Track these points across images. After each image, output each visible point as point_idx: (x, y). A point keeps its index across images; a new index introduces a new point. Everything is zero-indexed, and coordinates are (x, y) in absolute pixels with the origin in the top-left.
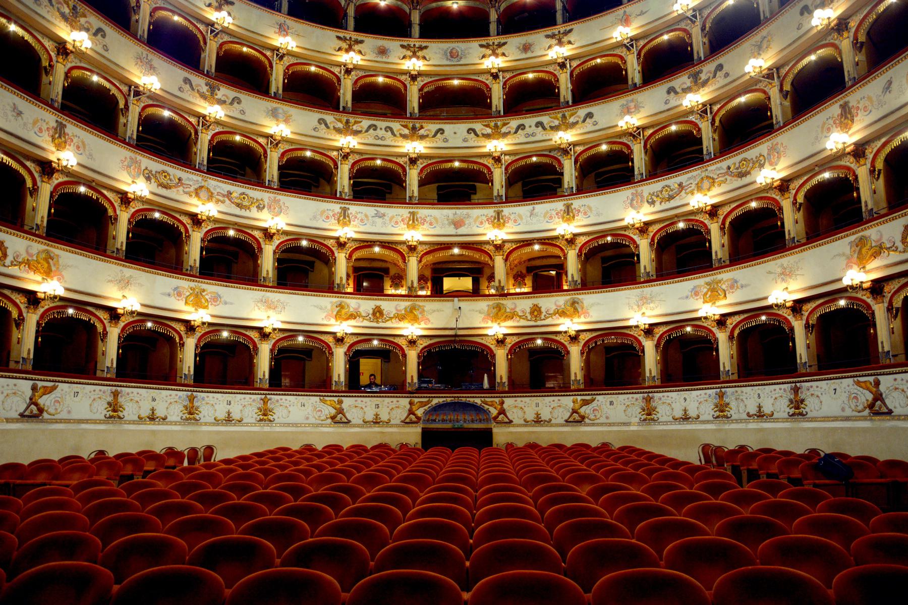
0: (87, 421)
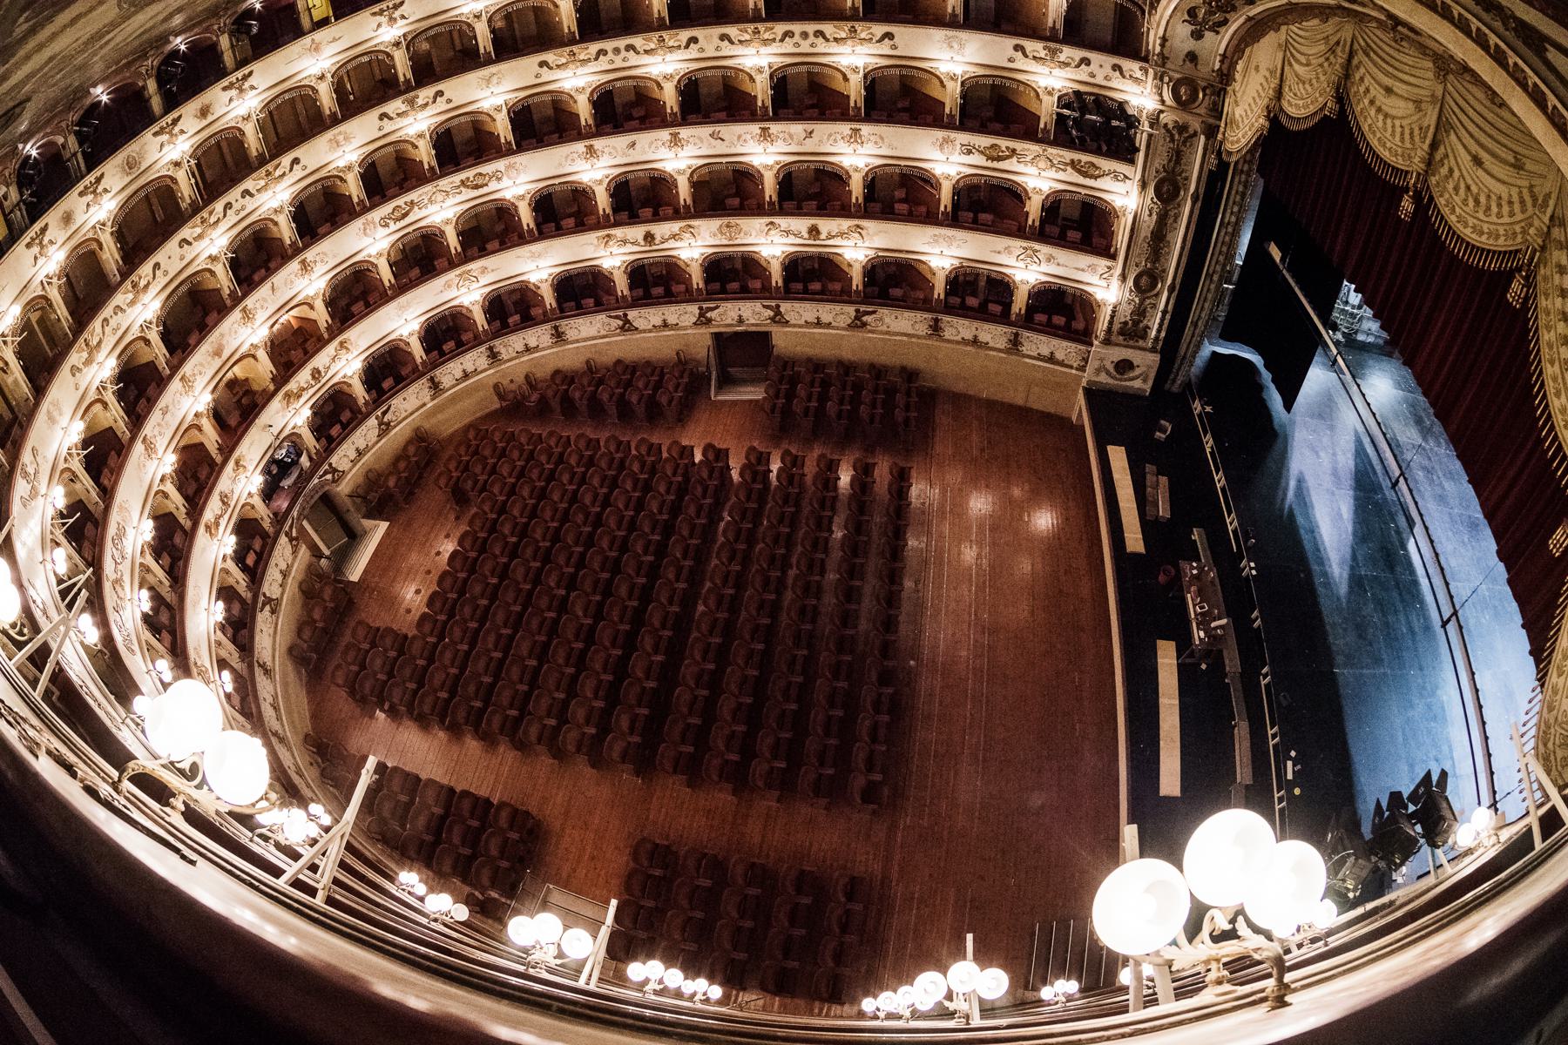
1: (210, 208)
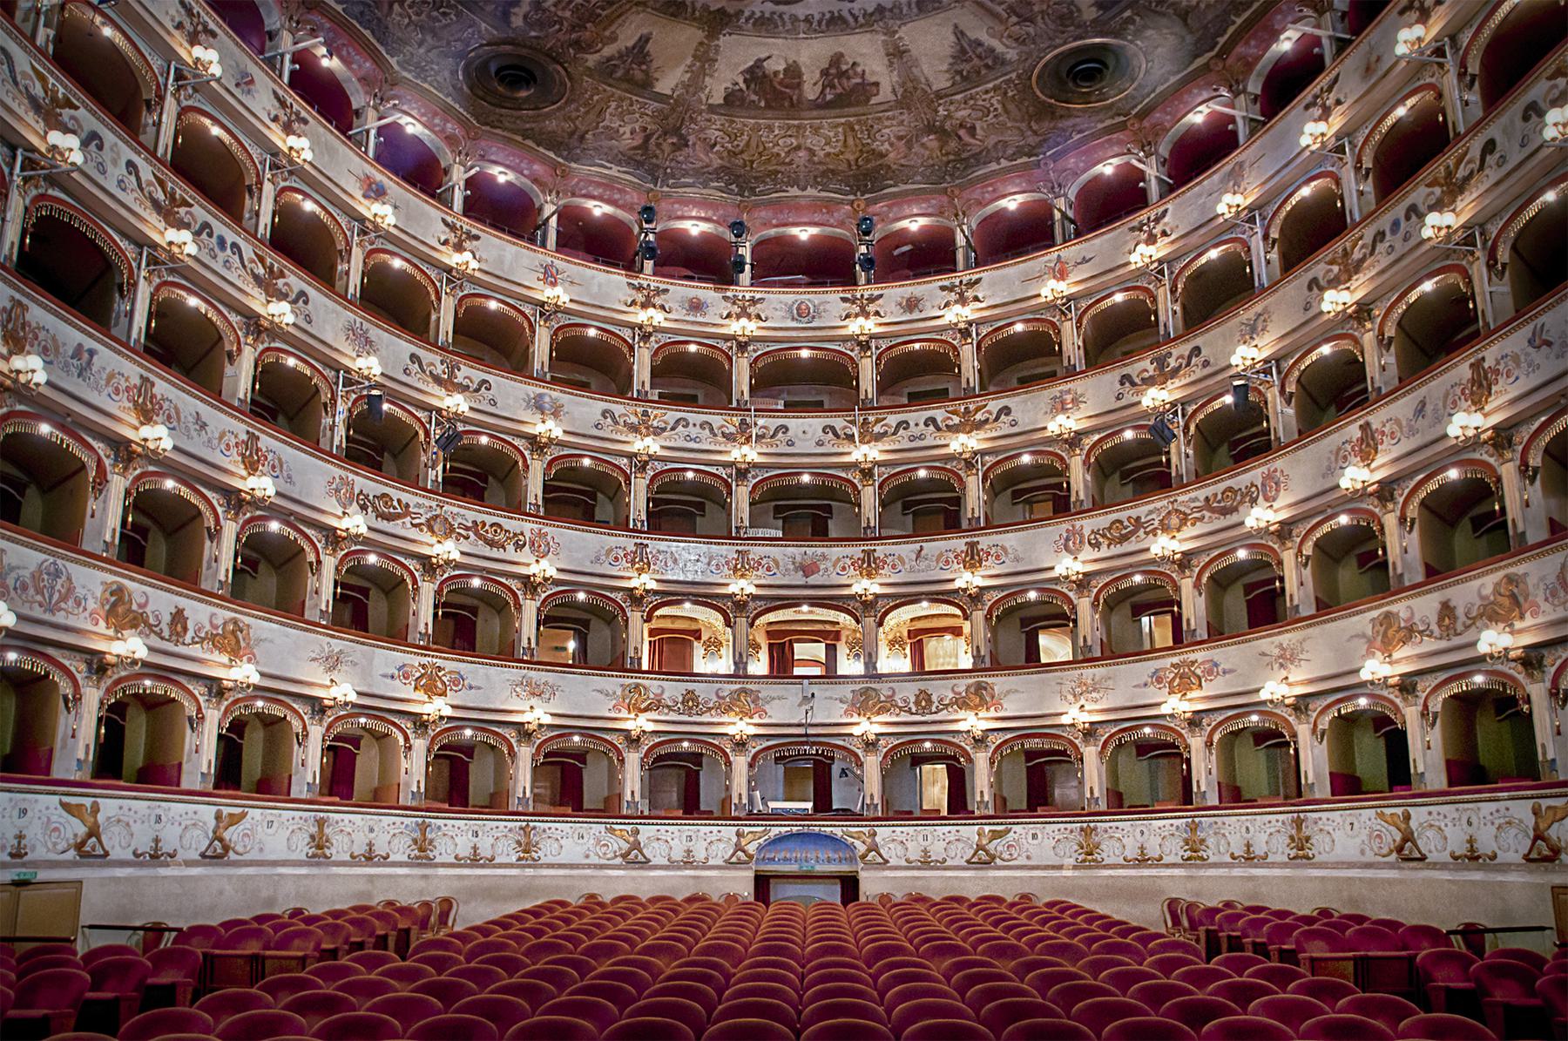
0: (284, 863)
1: (881, 414)
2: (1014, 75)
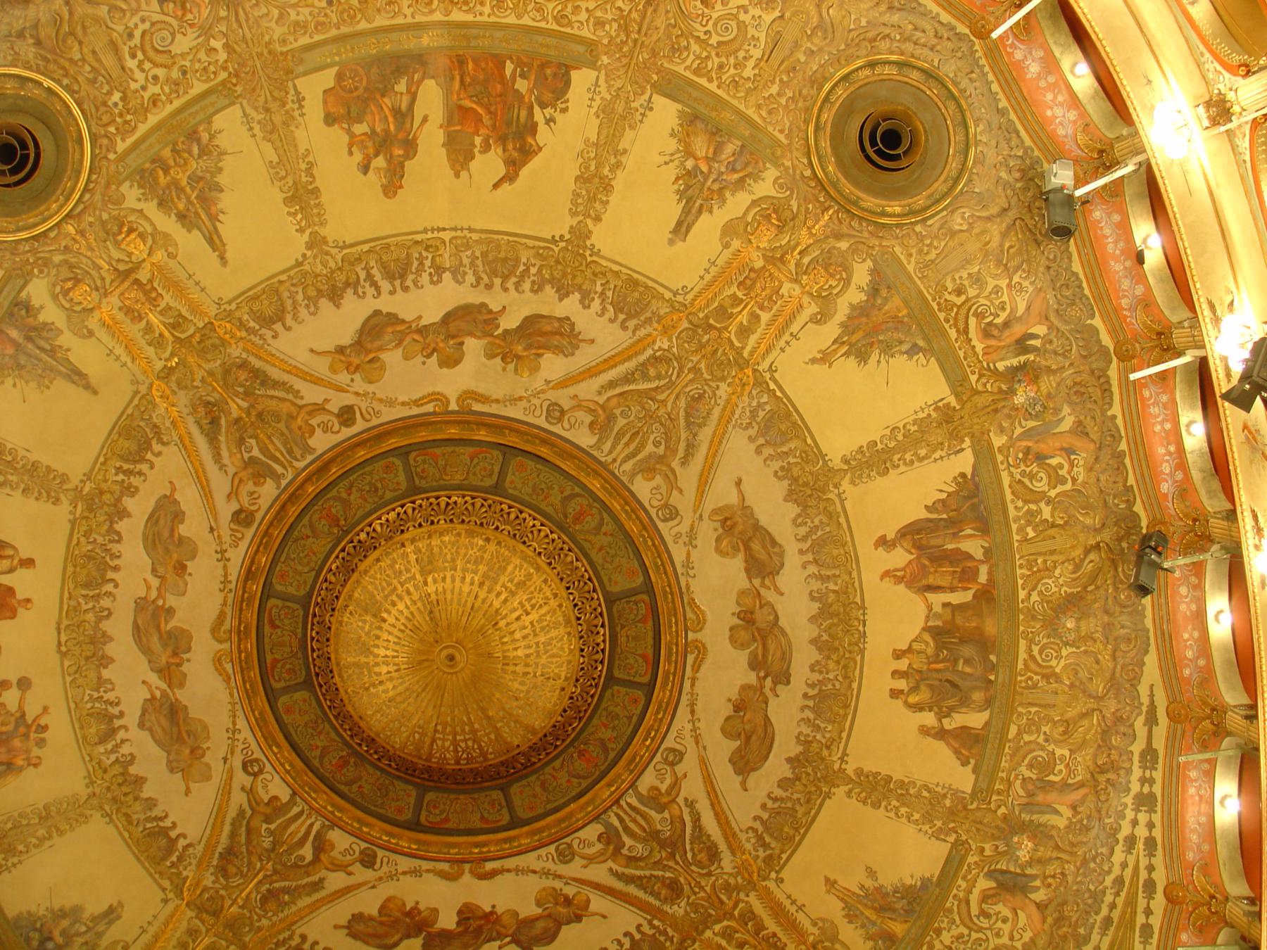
2: (121, 146)
